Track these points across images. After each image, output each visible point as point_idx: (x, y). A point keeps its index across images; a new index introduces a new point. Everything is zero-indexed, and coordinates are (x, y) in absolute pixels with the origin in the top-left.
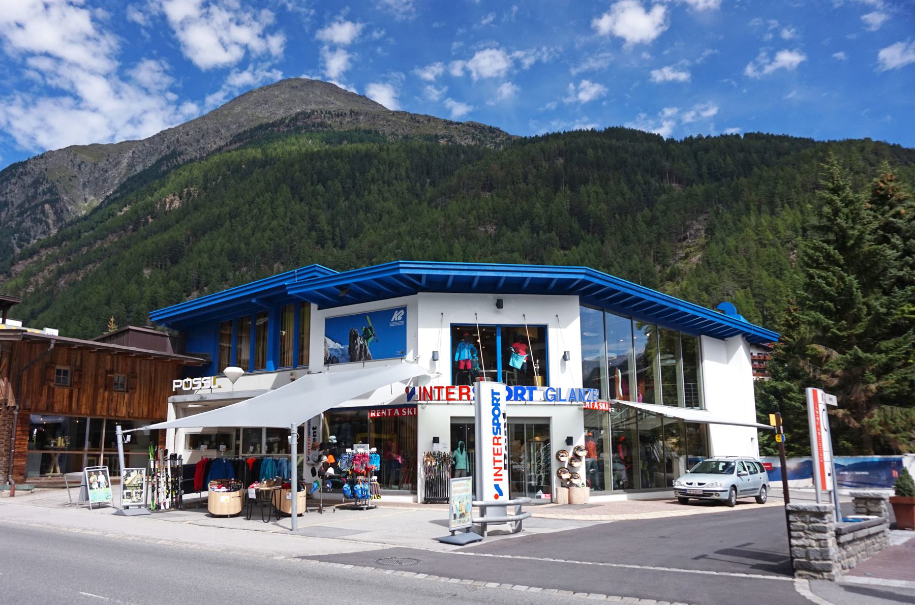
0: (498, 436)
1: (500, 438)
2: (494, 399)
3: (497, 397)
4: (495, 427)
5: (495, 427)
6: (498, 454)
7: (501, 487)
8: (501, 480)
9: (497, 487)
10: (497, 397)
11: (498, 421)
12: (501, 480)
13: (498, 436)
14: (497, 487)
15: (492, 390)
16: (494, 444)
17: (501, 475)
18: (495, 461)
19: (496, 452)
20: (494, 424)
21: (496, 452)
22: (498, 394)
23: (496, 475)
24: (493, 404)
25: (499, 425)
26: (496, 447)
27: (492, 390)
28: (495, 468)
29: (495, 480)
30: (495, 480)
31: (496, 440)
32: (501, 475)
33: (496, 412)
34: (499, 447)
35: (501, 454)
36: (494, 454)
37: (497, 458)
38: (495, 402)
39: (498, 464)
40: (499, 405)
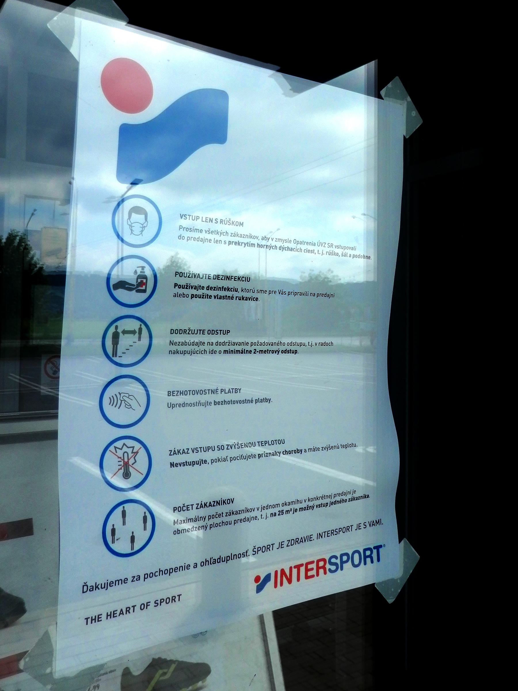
0: (328, 566)
6: (307, 570)
13: (328, 566)
14: (267, 578)
15: (381, 546)
16: (318, 561)
18: (298, 567)
19: (310, 566)
21: (310, 566)
23: (283, 571)
26: (314, 566)
31: (321, 564)
34: (314, 572)
36: (308, 564)
37: (303, 569)
39: (295, 571)
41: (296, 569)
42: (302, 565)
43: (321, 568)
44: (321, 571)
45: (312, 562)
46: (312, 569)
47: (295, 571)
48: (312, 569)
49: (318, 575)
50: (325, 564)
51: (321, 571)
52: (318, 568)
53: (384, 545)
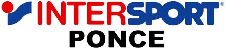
0: (126, 14)
1: (123, 23)
2: (200, 7)
3: (204, 18)
4: (144, 10)
5: (144, 10)
6: (90, 13)
7: (26, 18)
8: (40, 23)
9: (26, 9)
10: (204, 18)
11: (156, 17)
12: (40, 22)
13: (126, 14)
14: (26, 9)
15: (216, 5)
16: (110, 5)
17: (49, 23)
18: (76, 5)
19: (94, 8)
20: (150, 6)
21: (94, 8)
22: (211, 21)
23: (50, 6)
24: (190, 5)
25: (147, 18)
26: (104, 9)
27: (216, 5)
28: (63, 4)
29: (40, 4)
30: (40, 4)
32: (49, 23)
33: (173, 14)
34: (103, 18)
35: (90, 22)
36: (90, 5)
37: (83, 10)
38: (194, 11)
39: (70, 10)
40: (189, 23)
41: (72, 7)
42: (83, 4)
43: (115, 14)
44: (116, 19)
45: (102, 4)
46: (100, 13)
47: (70, 10)
48: (100, 13)
49: (109, 23)
50: (123, 10)
51: (116, 19)
52: (110, 14)
53: (223, 4)
